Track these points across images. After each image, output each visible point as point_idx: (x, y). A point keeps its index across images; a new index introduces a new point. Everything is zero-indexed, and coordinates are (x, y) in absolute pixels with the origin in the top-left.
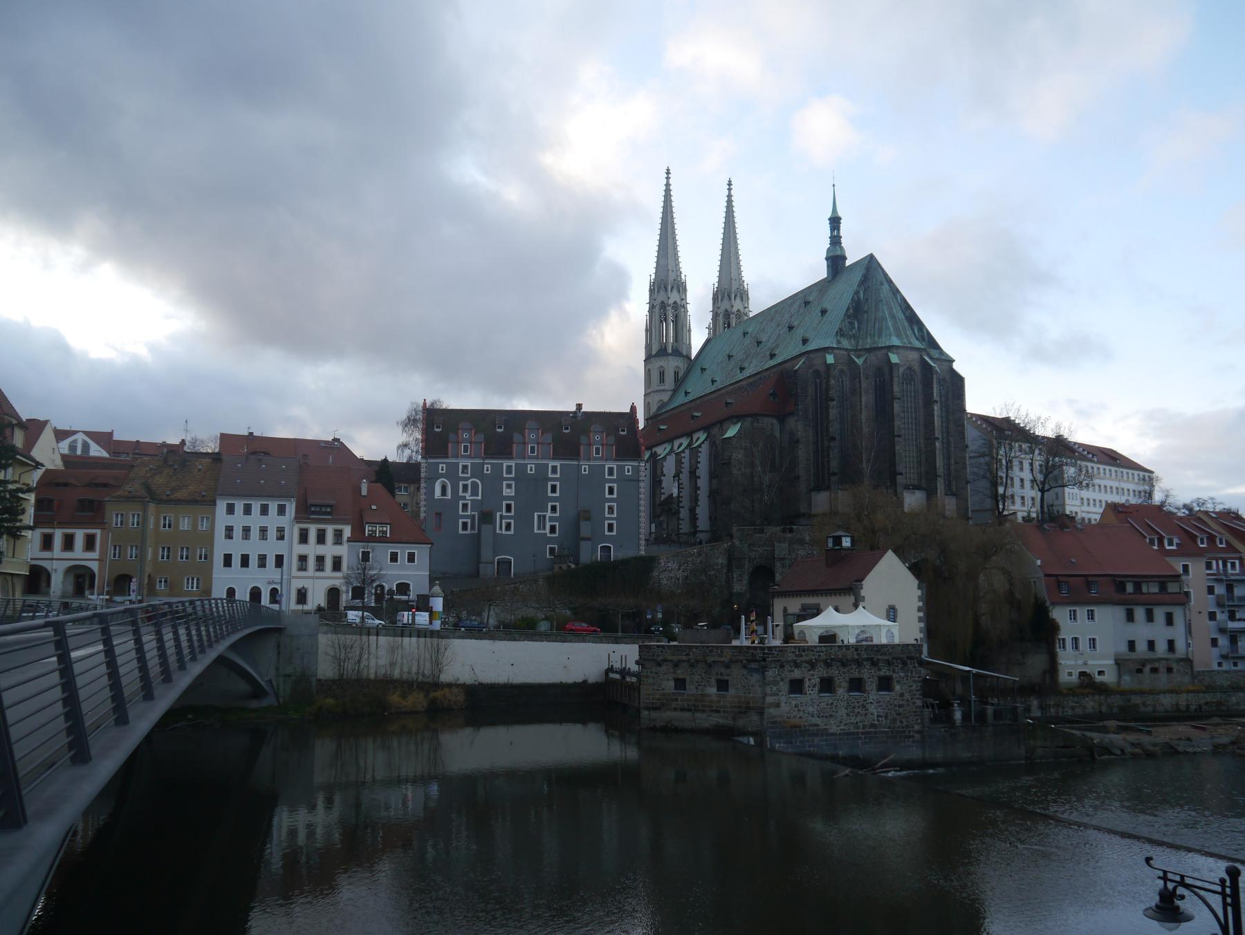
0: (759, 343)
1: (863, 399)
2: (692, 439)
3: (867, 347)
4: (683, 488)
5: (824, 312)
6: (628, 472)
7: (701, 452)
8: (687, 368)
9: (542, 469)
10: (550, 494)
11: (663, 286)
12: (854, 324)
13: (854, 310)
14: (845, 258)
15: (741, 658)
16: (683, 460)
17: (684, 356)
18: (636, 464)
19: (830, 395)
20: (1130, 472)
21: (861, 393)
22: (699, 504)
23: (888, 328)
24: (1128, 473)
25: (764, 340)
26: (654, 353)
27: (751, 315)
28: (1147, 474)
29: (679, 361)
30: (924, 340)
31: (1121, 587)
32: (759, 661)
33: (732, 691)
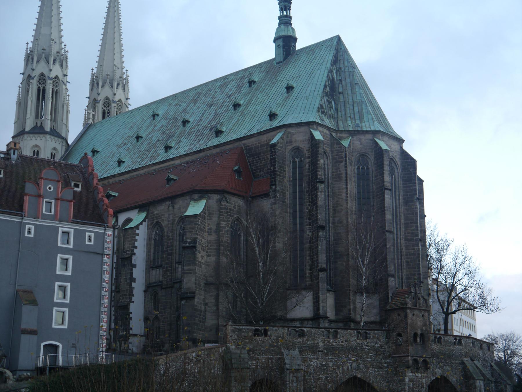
0: (185, 122)
1: (349, 187)
2: (117, 221)
3: (351, 129)
5: (289, 89)
6: (90, 240)
7: (138, 235)
8: (66, 151)
11: (44, 55)
12: (331, 102)
13: (330, 89)
14: (295, 40)
17: (62, 138)
18: (100, 230)
19: (319, 177)
21: (347, 180)
22: (133, 300)
23: (368, 112)
25: (191, 120)
26: (28, 129)
27: (130, 108)
29: (57, 143)
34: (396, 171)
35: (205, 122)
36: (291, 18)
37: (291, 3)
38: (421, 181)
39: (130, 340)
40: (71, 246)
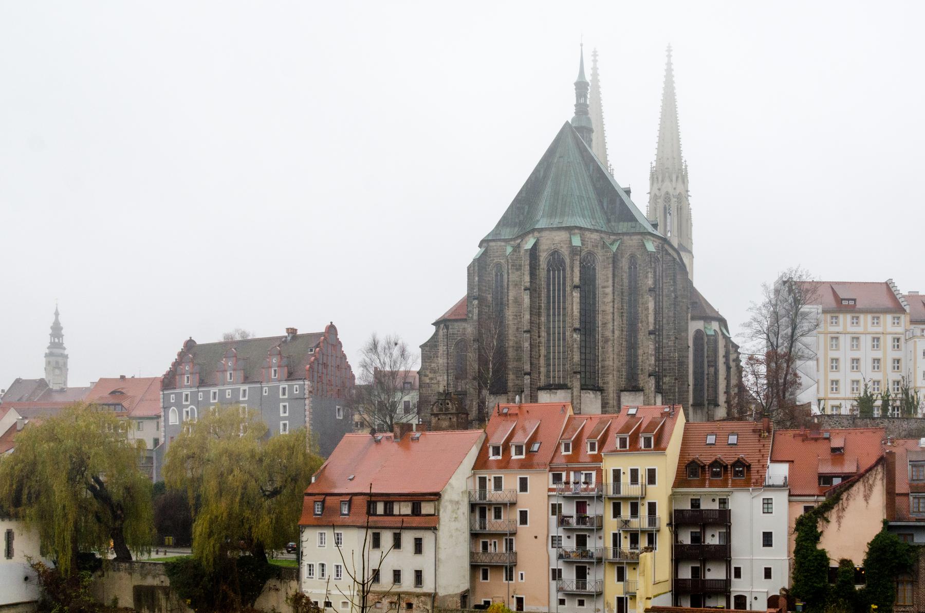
9: (235, 392)
18: (301, 382)
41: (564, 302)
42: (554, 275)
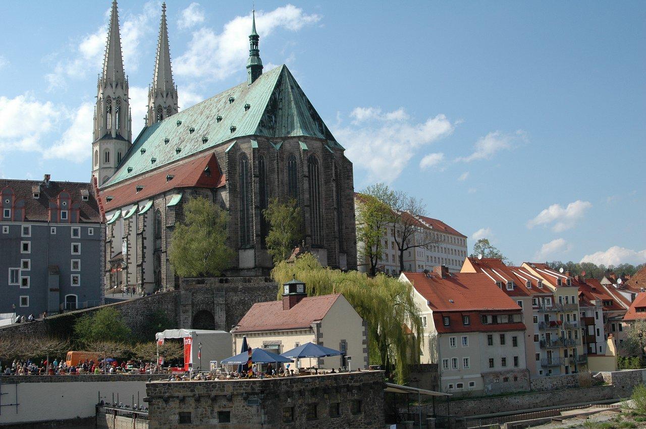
0: (192, 131)
2: (138, 207)
3: (283, 136)
4: (130, 247)
5: (247, 107)
6: (91, 233)
7: (147, 218)
9: (15, 229)
10: (22, 252)
14: (261, 67)
15: (242, 391)
16: (131, 224)
18: (97, 226)
20: (453, 236)
21: (278, 172)
24: (451, 238)
28: (463, 239)
30: (322, 133)
31: (485, 318)
32: (257, 394)
33: (233, 421)
34: (319, 161)
35: (201, 132)
36: (258, 51)
37: (258, 40)
38: (350, 164)
39: (144, 286)
40: (80, 237)
41: (319, 188)
42: (312, 167)
